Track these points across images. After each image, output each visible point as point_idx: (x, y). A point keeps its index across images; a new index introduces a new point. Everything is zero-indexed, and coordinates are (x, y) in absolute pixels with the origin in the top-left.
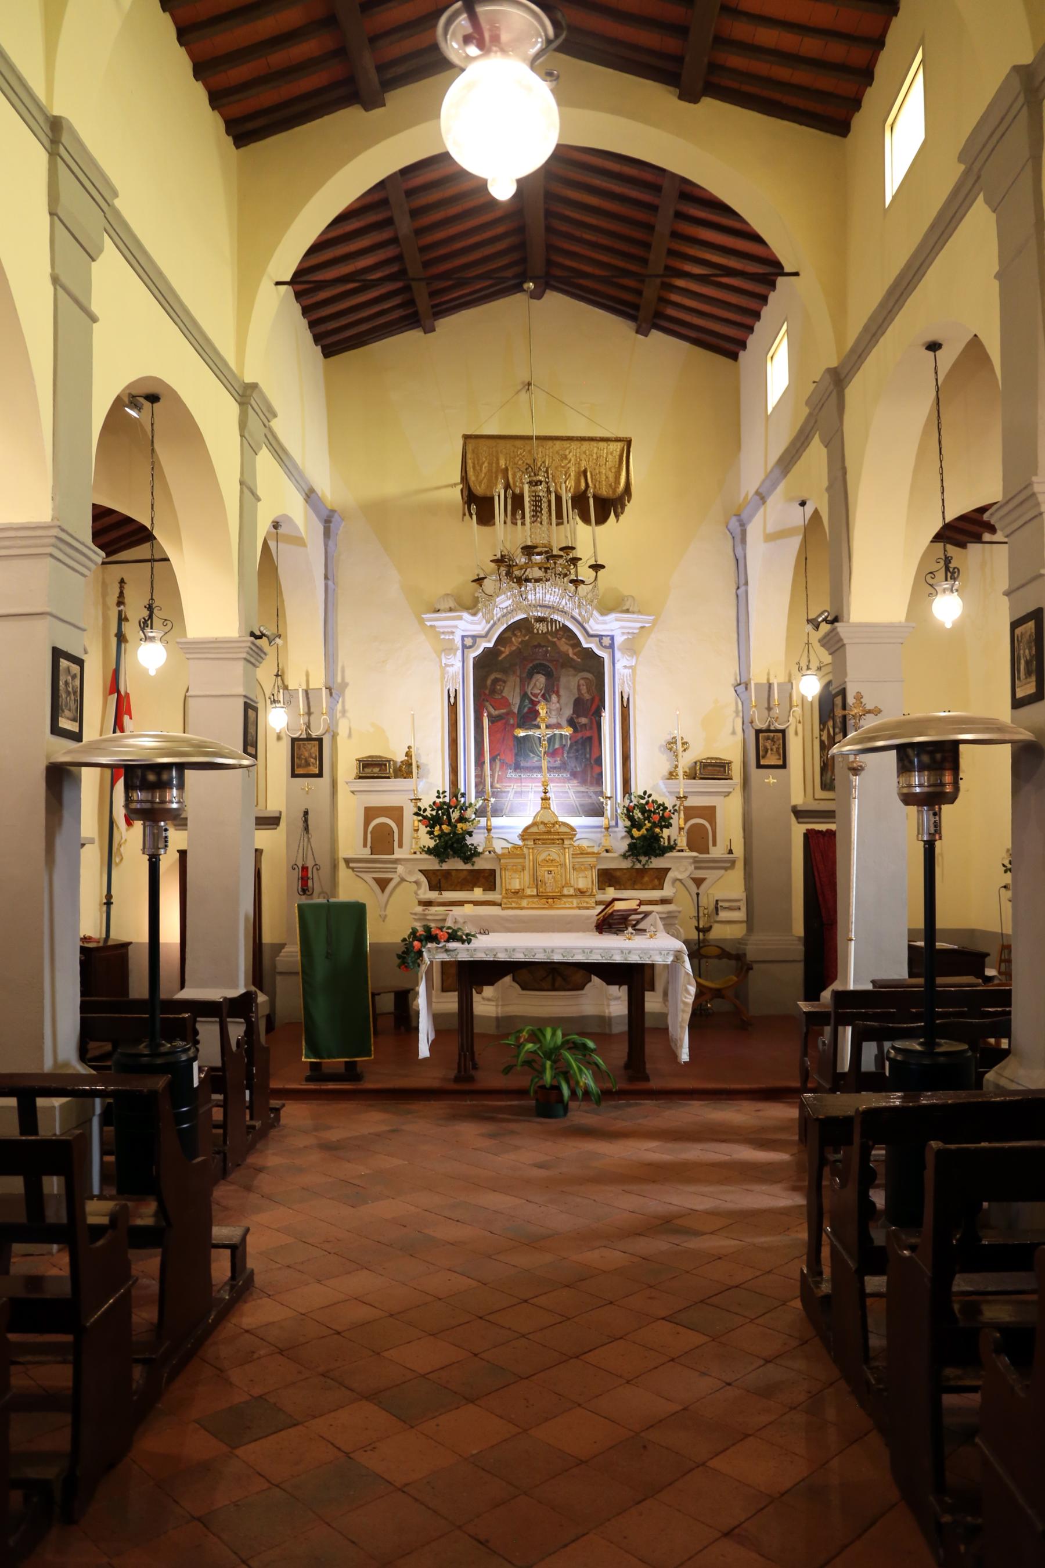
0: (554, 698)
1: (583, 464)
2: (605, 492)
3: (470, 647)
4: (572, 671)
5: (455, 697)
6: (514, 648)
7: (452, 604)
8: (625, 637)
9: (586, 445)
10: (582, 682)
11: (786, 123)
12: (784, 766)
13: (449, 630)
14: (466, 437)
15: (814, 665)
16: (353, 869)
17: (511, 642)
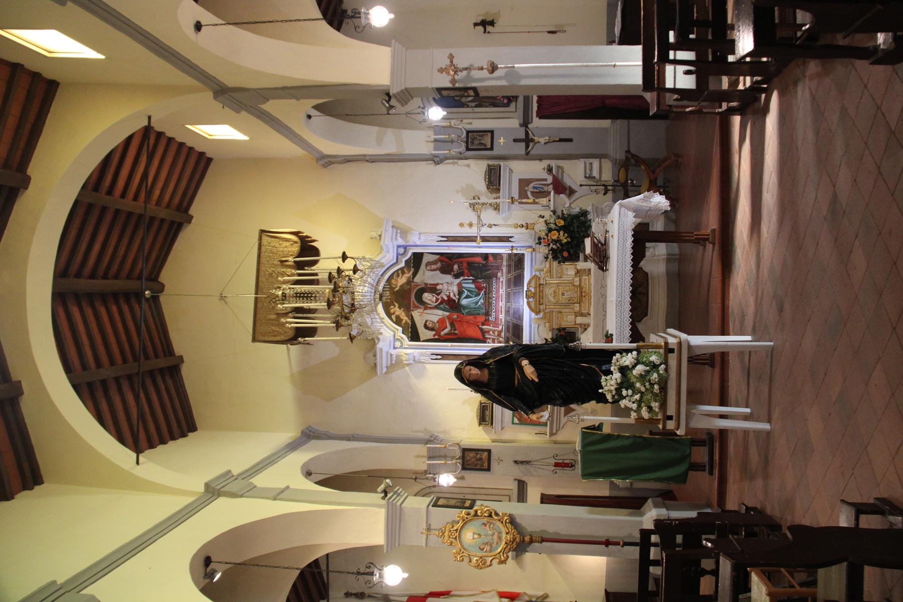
0: (438, 287)
1: (276, 262)
2: (296, 249)
7: (371, 355)
8: (399, 238)
9: (263, 260)
11: (47, 122)
12: (492, 132)
14: (254, 340)
15: (421, 110)
16: (557, 431)
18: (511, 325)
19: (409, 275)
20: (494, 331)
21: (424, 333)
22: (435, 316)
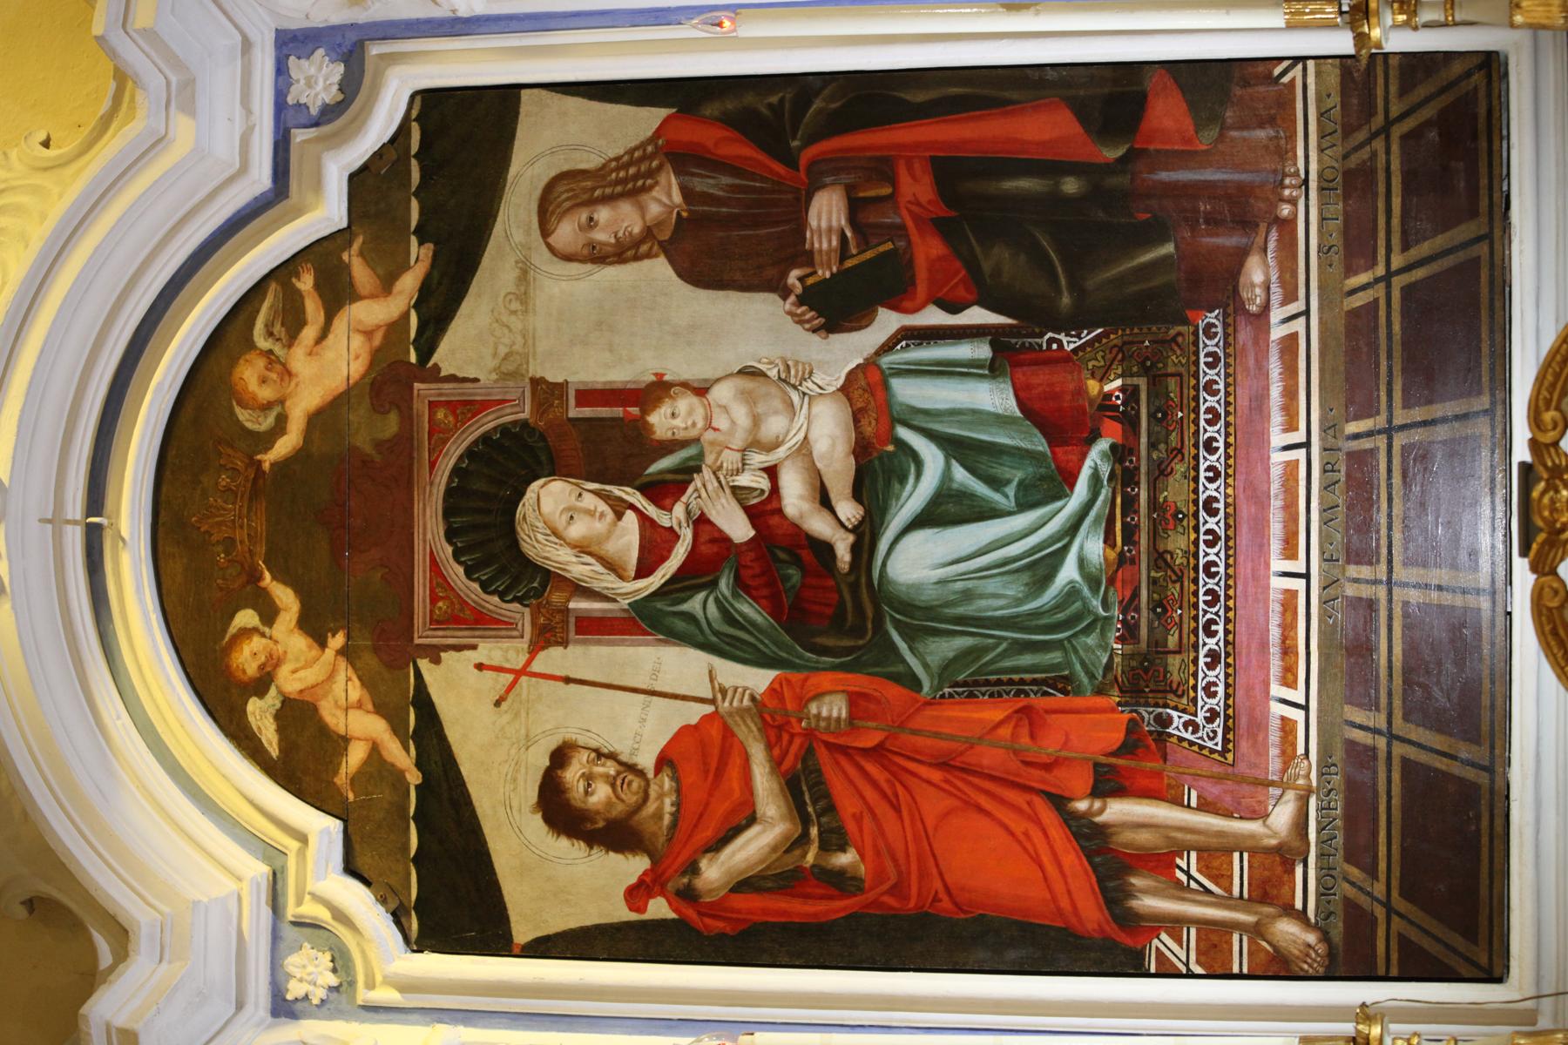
0: (664, 421)
10: (566, 232)
18: (1389, 787)
19: (380, 309)
20: (1215, 854)
21: (549, 876)
22: (641, 700)
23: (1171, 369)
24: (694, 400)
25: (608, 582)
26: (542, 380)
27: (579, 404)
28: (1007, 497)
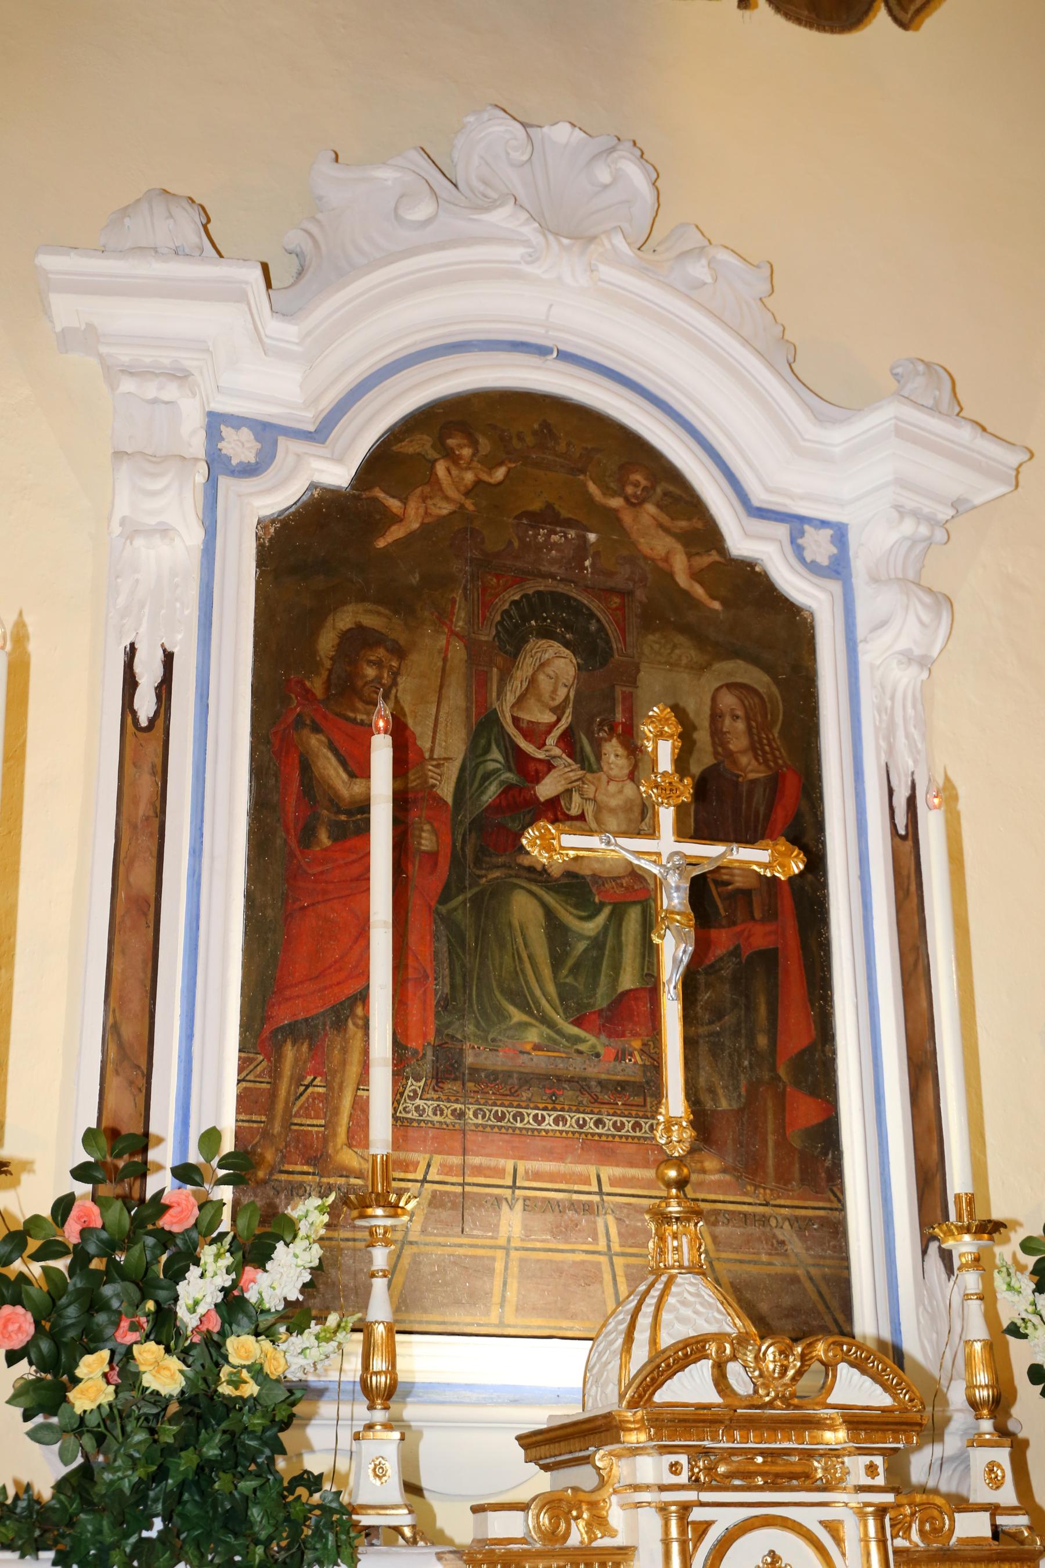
3: (248, 471)
4: (687, 652)
5: (164, 689)
6: (445, 509)
10: (728, 700)
13: (166, 358)
17: (432, 479)
23: (648, 1099)
24: (626, 771)
25: (510, 698)
26: (638, 671)
27: (623, 693)
28: (566, 977)
